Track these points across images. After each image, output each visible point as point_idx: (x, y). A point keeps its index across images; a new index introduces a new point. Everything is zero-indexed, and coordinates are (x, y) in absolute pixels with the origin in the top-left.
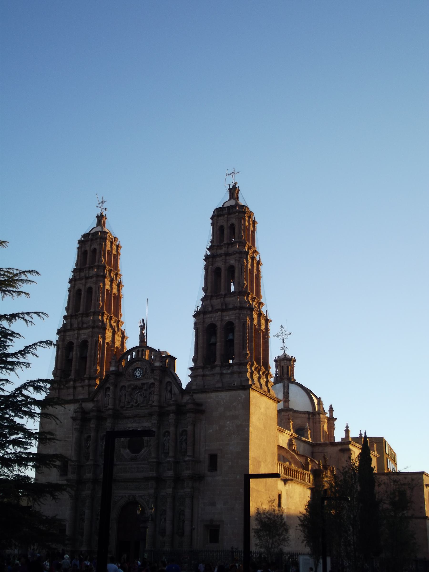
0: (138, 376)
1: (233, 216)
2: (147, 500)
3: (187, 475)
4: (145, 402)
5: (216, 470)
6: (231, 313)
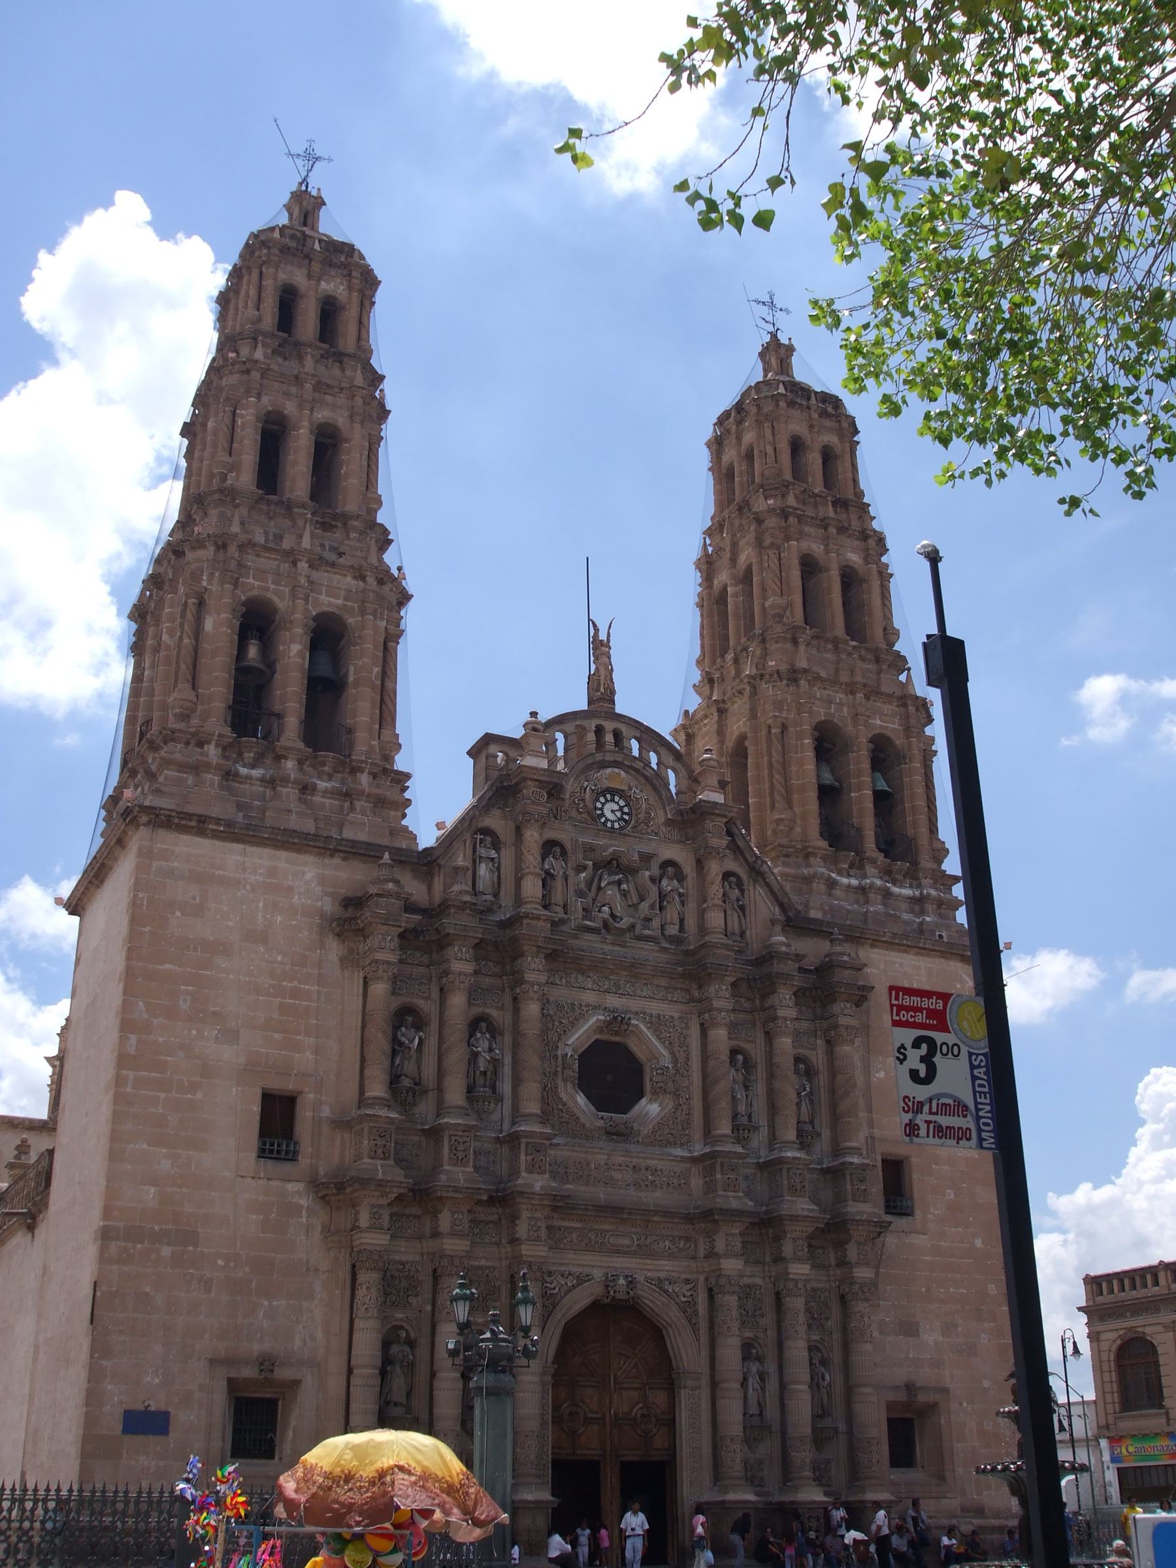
0: (613, 822)
1: (828, 423)
2: (684, 1299)
3: (865, 1217)
4: (656, 923)
5: (907, 1213)
6: (888, 708)
